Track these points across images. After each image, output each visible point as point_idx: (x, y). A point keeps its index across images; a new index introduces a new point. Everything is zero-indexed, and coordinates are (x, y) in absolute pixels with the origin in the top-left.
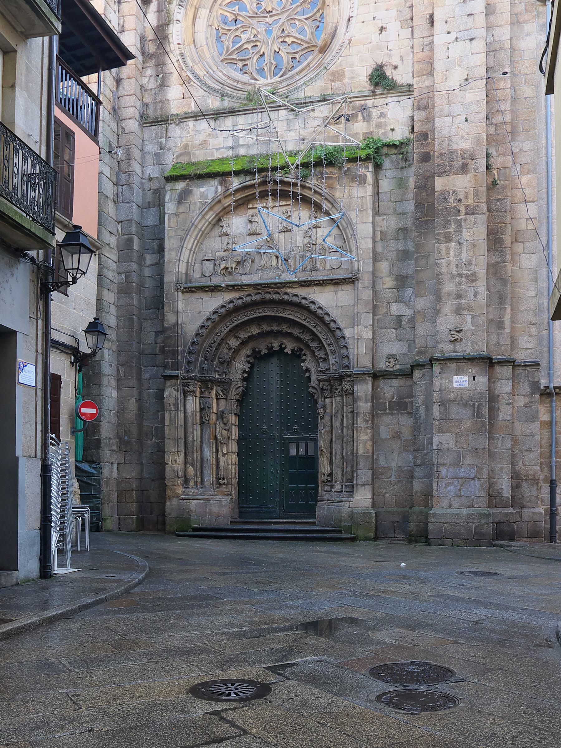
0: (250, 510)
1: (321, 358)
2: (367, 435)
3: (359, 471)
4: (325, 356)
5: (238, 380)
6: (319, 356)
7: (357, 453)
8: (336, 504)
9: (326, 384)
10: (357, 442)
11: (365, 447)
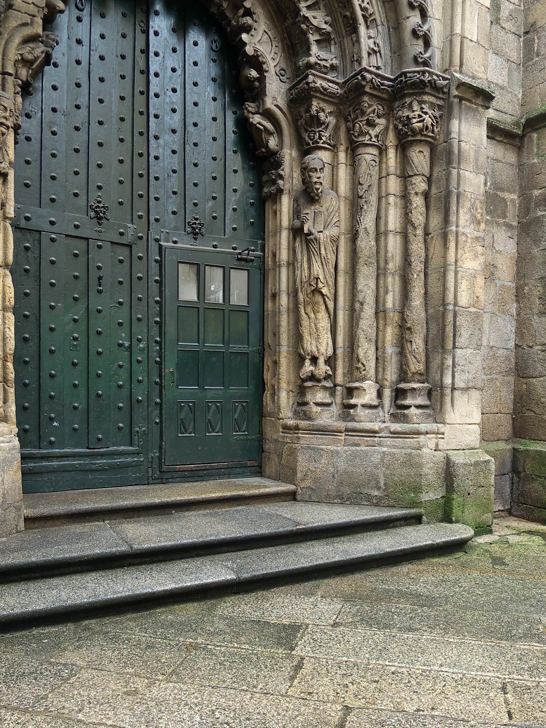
0: (55, 463)
1: (318, 30)
2: (476, 256)
3: (458, 352)
4: (328, 28)
5: (32, 9)
6: (315, 22)
7: (455, 305)
8: (389, 441)
9: (328, 108)
10: (456, 273)
11: (472, 288)
